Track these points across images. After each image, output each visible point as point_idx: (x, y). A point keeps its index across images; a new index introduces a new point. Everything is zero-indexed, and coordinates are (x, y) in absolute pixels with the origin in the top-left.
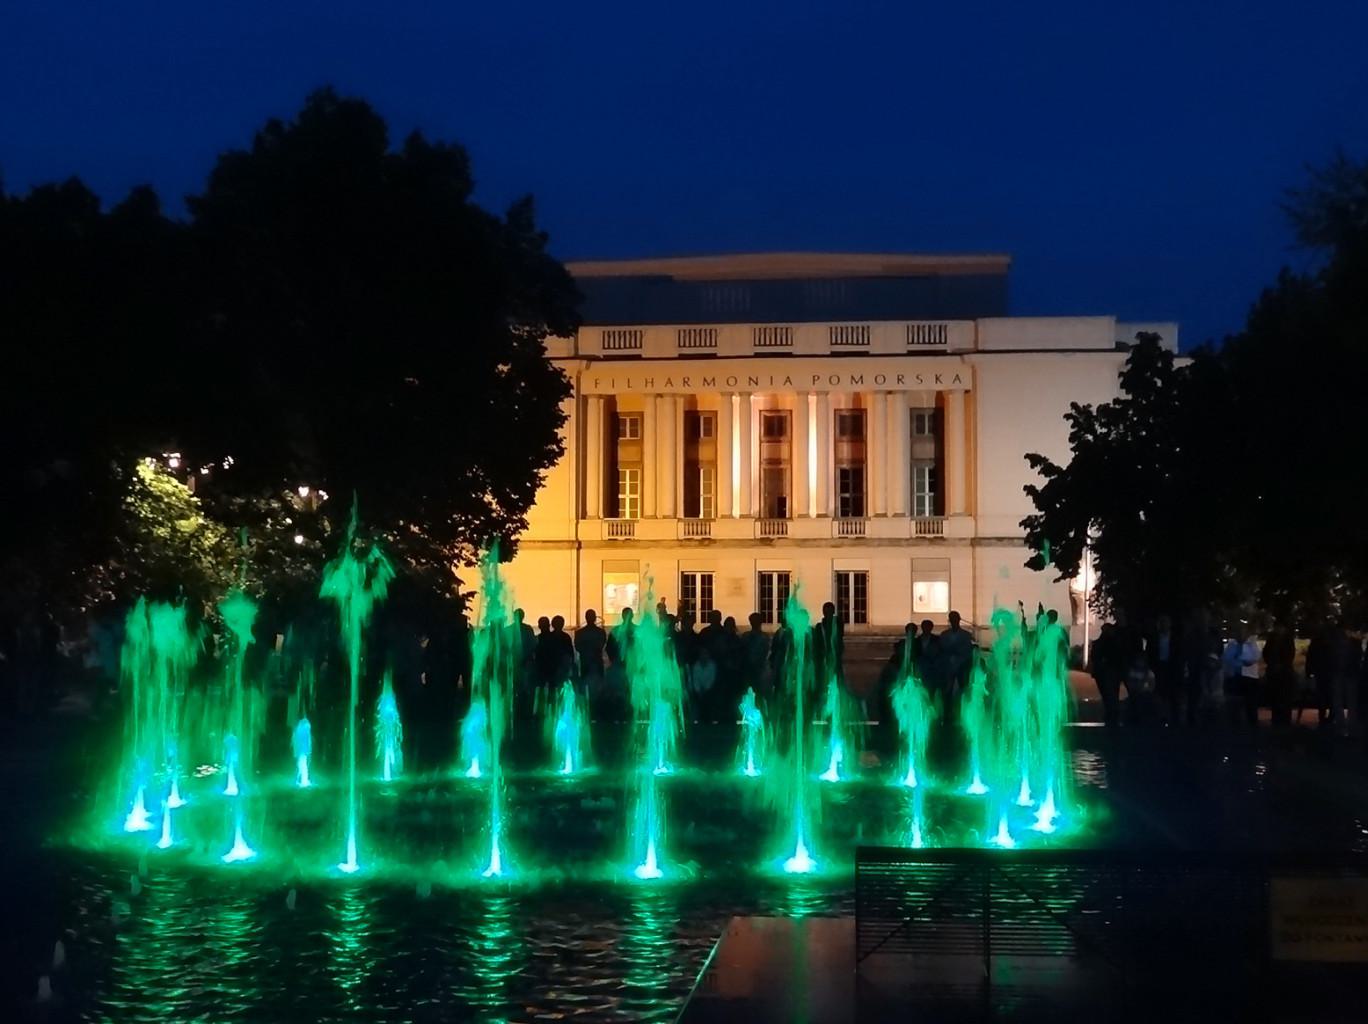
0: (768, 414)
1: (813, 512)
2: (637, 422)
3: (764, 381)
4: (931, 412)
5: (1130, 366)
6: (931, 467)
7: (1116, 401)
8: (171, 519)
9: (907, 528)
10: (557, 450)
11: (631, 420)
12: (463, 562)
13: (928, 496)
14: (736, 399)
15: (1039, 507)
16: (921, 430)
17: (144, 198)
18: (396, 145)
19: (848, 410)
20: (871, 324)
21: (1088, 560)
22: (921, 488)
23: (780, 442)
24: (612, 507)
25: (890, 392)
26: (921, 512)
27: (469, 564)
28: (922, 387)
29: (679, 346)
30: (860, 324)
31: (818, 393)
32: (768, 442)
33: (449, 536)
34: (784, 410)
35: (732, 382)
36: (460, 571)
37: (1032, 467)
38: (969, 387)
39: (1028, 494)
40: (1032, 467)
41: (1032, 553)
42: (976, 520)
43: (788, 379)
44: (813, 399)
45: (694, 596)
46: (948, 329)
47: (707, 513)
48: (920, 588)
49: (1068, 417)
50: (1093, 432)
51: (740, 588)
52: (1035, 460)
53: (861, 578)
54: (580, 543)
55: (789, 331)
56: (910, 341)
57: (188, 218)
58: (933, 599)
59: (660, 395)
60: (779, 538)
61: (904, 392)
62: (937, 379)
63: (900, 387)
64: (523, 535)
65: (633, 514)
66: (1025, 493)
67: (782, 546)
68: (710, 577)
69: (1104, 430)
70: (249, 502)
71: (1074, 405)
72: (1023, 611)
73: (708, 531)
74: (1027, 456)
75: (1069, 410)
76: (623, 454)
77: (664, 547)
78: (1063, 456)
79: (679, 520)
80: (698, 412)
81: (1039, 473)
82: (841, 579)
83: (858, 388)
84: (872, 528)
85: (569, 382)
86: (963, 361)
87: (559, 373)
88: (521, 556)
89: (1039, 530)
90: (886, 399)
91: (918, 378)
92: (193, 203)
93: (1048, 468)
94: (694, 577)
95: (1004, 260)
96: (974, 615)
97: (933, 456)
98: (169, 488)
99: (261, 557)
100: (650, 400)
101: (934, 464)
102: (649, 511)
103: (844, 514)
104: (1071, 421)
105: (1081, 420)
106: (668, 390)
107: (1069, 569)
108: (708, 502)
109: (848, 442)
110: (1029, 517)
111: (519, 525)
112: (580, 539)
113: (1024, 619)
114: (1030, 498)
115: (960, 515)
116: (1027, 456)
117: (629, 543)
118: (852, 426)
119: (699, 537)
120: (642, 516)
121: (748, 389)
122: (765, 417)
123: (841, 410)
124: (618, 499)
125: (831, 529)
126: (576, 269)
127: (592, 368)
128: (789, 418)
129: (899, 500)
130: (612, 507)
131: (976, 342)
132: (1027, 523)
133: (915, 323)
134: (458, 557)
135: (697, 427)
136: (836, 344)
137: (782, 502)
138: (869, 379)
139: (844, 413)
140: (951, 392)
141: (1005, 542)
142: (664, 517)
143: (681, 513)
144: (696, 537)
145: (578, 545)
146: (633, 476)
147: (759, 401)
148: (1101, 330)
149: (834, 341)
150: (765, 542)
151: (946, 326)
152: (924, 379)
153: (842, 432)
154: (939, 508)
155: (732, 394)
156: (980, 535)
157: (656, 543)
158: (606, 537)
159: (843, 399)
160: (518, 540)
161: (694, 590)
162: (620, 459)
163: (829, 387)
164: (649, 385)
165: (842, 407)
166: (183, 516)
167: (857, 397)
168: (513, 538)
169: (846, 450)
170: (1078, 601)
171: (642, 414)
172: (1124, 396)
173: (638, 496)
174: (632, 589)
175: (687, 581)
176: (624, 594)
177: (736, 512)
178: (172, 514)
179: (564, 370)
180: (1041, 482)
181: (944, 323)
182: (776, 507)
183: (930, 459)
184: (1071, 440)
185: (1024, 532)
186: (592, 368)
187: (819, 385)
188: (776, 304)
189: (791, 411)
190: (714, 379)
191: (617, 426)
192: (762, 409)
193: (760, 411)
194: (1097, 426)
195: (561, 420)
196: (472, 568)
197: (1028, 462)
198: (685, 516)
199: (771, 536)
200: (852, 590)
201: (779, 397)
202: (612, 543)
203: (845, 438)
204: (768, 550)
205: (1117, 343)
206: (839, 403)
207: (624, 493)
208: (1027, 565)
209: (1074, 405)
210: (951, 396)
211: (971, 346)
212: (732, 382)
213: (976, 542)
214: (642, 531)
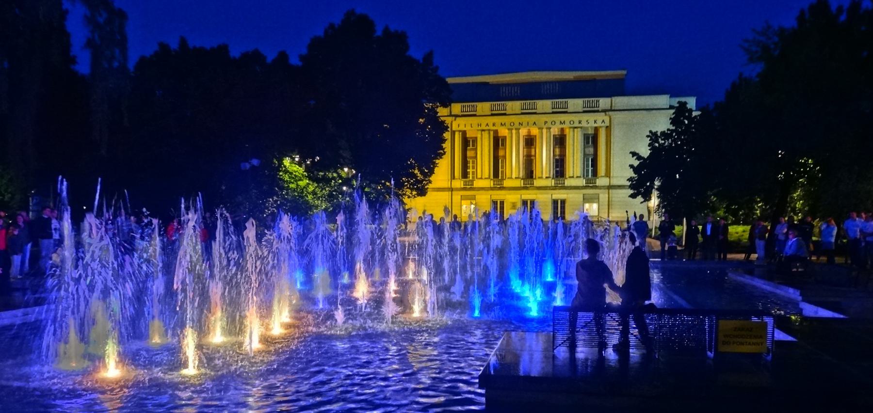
1: (544, 176)
2: (475, 140)
7: (668, 130)
8: (296, 181)
9: (582, 182)
13: (590, 169)
14: (514, 131)
15: (635, 173)
16: (588, 143)
17: (283, 56)
18: (379, 32)
21: (655, 194)
22: (588, 166)
24: (465, 175)
26: (588, 175)
27: (409, 197)
33: (400, 185)
36: (406, 200)
41: (632, 192)
44: (545, 131)
47: (502, 177)
48: (587, 206)
49: (648, 136)
50: (658, 142)
52: (634, 154)
53: (563, 202)
57: (300, 64)
58: (592, 209)
62: (595, 122)
64: (430, 186)
71: (651, 132)
76: (470, 154)
78: (645, 152)
82: (555, 202)
83: (562, 126)
84: (568, 182)
87: (443, 122)
88: (429, 193)
92: (302, 58)
98: (295, 169)
99: (330, 195)
102: (479, 176)
103: (557, 177)
106: (487, 128)
107: (647, 197)
108: (502, 172)
118: (560, 141)
125: (551, 182)
126: (450, 80)
127: (458, 120)
129: (578, 171)
130: (465, 175)
134: (405, 194)
135: (498, 142)
137: (532, 172)
138: (567, 123)
145: (451, 190)
146: (473, 163)
147: (523, 132)
148: (663, 100)
152: (591, 121)
154: (595, 173)
166: (300, 180)
167: (562, 130)
169: (557, 151)
175: (495, 203)
177: (514, 176)
178: (297, 179)
180: (636, 163)
182: (529, 174)
184: (649, 145)
185: (629, 183)
186: (458, 120)
188: (530, 92)
191: (466, 142)
195: (444, 141)
200: (559, 207)
202: (464, 189)
209: (651, 132)
213: (610, 187)
214: (478, 184)
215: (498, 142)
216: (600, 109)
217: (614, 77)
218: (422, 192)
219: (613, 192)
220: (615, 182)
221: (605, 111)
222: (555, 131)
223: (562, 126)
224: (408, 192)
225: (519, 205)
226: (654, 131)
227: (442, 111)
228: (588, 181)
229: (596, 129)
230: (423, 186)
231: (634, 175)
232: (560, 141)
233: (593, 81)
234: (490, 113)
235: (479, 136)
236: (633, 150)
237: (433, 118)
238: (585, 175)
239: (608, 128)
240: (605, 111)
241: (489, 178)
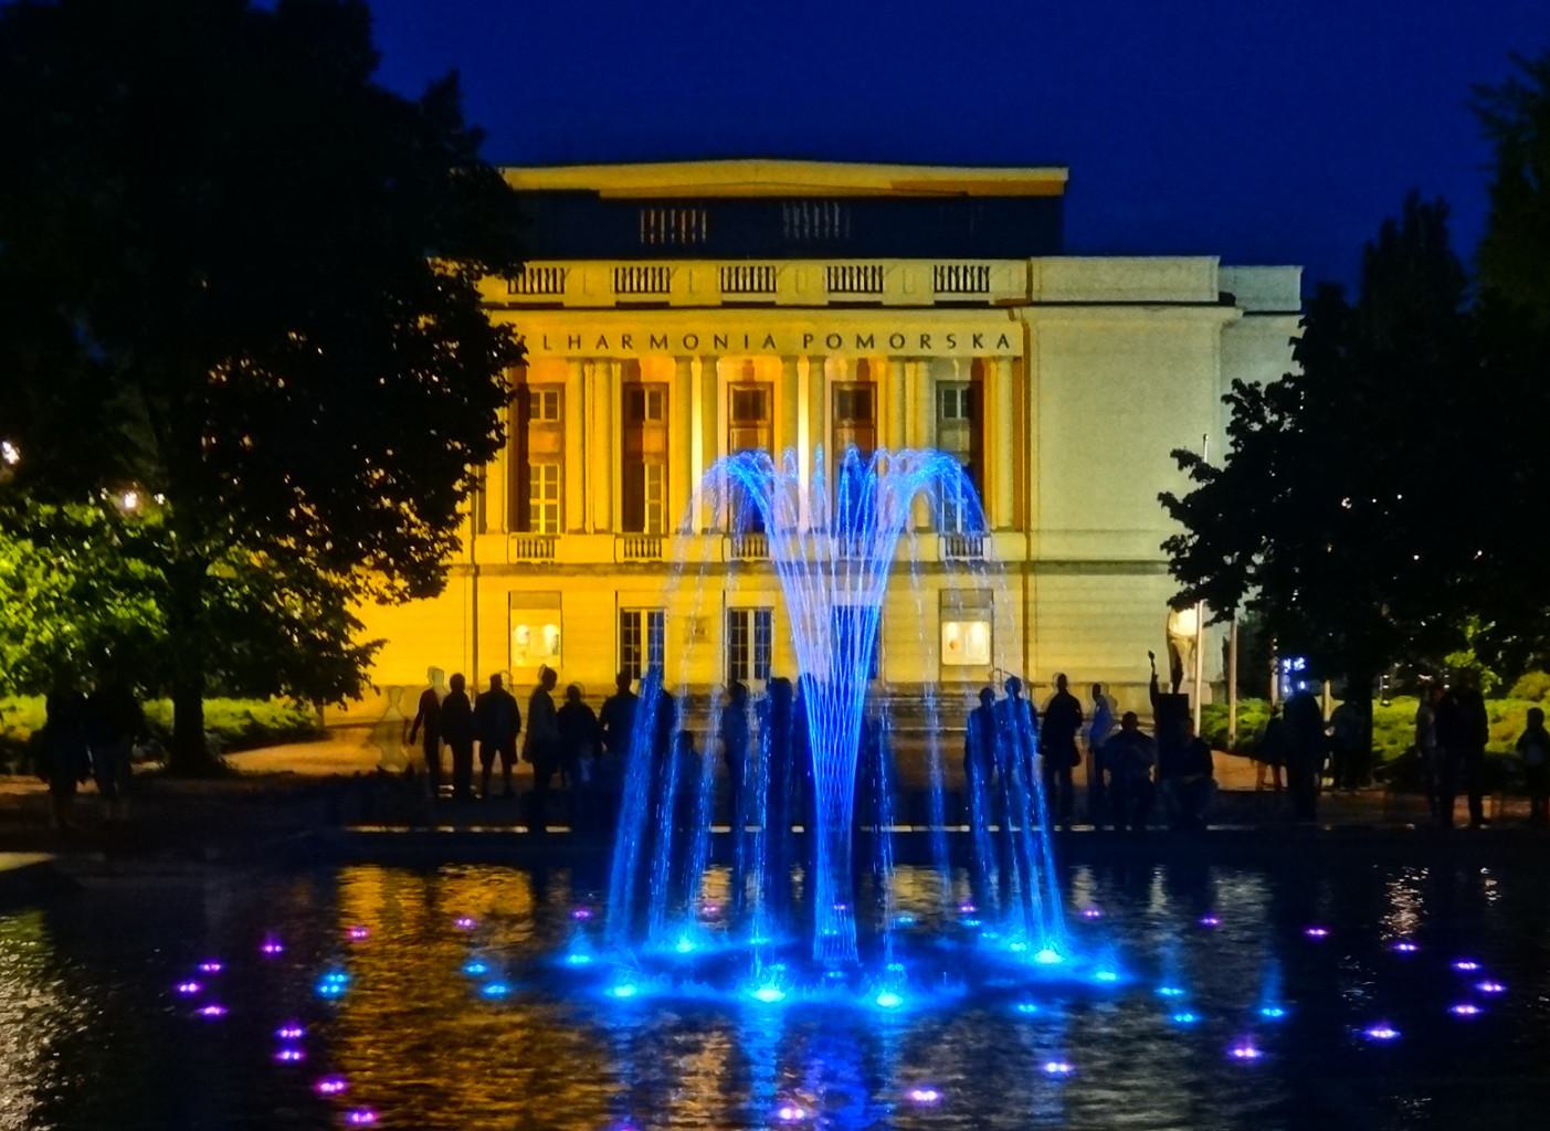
0: (739, 388)
2: (556, 395)
3: (736, 342)
4: (965, 388)
5: (1304, 328)
6: (966, 464)
7: (1287, 377)
9: (931, 547)
10: (497, 440)
11: (547, 395)
12: (373, 598)
14: (697, 367)
16: (951, 412)
19: (850, 383)
20: (886, 263)
23: (756, 427)
24: (520, 517)
25: (909, 359)
26: (951, 525)
27: (382, 600)
28: (953, 353)
29: (617, 291)
30: (869, 263)
31: (811, 359)
32: (741, 427)
33: (341, 560)
34: (762, 383)
35: (691, 341)
36: (360, 607)
37: (1180, 468)
38: (1020, 353)
39: (1164, 505)
40: (1180, 468)
42: (1028, 538)
43: (769, 340)
44: (803, 367)
45: (638, 641)
46: (991, 272)
47: (655, 527)
48: (951, 630)
49: (1227, 399)
50: (1262, 420)
51: (703, 632)
52: (1184, 458)
54: (477, 568)
55: (771, 271)
56: (939, 288)
58: (971, 646)
59: (591, 361)
60: (756, 562)
61: (929, 359)
62: (976, 341)
63: (926, 352)
64: (456, 558)
65: (550, 527)
66: (1160, 503)
67: (760, 572)
68: (661, 616)
69: (1275, 418)
70: (60, 513)
71: (1237, 384)
72: (1153, 665)
73: (657, 551)
74: (1175, 454)
75: (1229, 390)
77: (595, 573)
78: (1216, 450)
79: (617, 536)
80: (639, 384)
81: (1190, 477)
84: (886, 550)
85: (521, 343)
86: (1012, 318)
87: (507, 330)
88: (456, 587)
89: (1187, 555)
90: (903, 372)
91: (949, 339)
93: (1202, 471)
94: (637, 616)
95: (1051, 177)
96: (1026, 666)
97: (967, 448)
99: (84, 596)
100: (575, 367)
101: (969, 460)
102: (574, 521)
104: (1232, 406)
105: (1245, 404)
106: (602, 352)
108: (655, 510)
109: (850, 427)
110: (1173, 538)
111: (448, 545)
112: (477, 561)
113: (1154, 677)
114: (1167, 510)
115: (1000, 529)
116: (1175, 454)
117: (542, 569)
118: (856, 405)
119: (645, 560)
120: (563, 530)
121: (713, 352)
122: (735, 392)
123: (842, 383)
124: (528, 506)
127: (567, 328)
128: (768, 394)
130: (520, 517)
131: (1029, 291)
132: (1172, 544)
133: (946, 263)
134: (357, 589)
135: (639, 404)
136: (836, 290)
139: (847, 388)
140: (997, 359)
141: (1068, 567)
142: (597, 532)
143: (618, 528)
144: (641, 560)
146: (551, 473)
147: (729, 370)
148: (1198, 274)
149: (833, 287)
150: (741, 567)
151: (988, 269)
152: (959, 338)
153: (843, 414)
154: (977, 519)
155: (690, 359)
156: (1034, 555)
157: (587, 569)
158: (514, 559)
159: (843, 365)
160: (448, 567)
161: (638, 634)
162: (531, 449)
163: (827, 351)
164: (575, 346)
165: (843, 377)
167: (863, 366)
168: (442, 562)
170: (1179, 649)
171: (562, 386)
172: (1297, 370)
173: (557, 502)
174: (551, 632)
176: (541, 637)
177: (697, 526)
179: (514, 326)
180: (1184, 485)
181: (985, 263)
183: (963, 452)
184: (1229, 431)
186: (567, 328)
187: (812, 349)
189: (771, 385)
190: (665, 338)
192: (731, 380)
193: (729, 384)
194: (1267, 411)
196: (387, 606)
197: (1176, 461)
198: (624, 530)
199: (746, 559)
200: (855, 635)
201: (755, 365)
202: (523, 568)
203: (846, 423)
204: (744, 580)
205: (1222, 295)
206: (838, 370)
207: (538, 496)
208: (1169, 603)
209: (1237, 384)
210: (993, 366)
211: (1024, 296)
212: (691, 341)
213: (1029, 567)
215: (639, 404)
216: (990, 298)
217: (1019, 192)
218: (426, 582)
219: (1043, 583)
220: (1046, 548)
221: (1006, 305)
222: (840, 368)
223: (868, 353)
224: (379, 580)
225: (719, 632)
226: (1246, 382)
227: (492, 288)
228: (956, 545)
229: (978, 366)
230: (431, 563)
231: (1179, 528)
232: (856, 405)
233: (958, 204)
234: (611, 300)
235: (572, 380)
236: (1180, 447)
237: (465, 313)
238: (941, 521)
239: (1021, 366)
240: (1006, 305)
241: (609, 531)
